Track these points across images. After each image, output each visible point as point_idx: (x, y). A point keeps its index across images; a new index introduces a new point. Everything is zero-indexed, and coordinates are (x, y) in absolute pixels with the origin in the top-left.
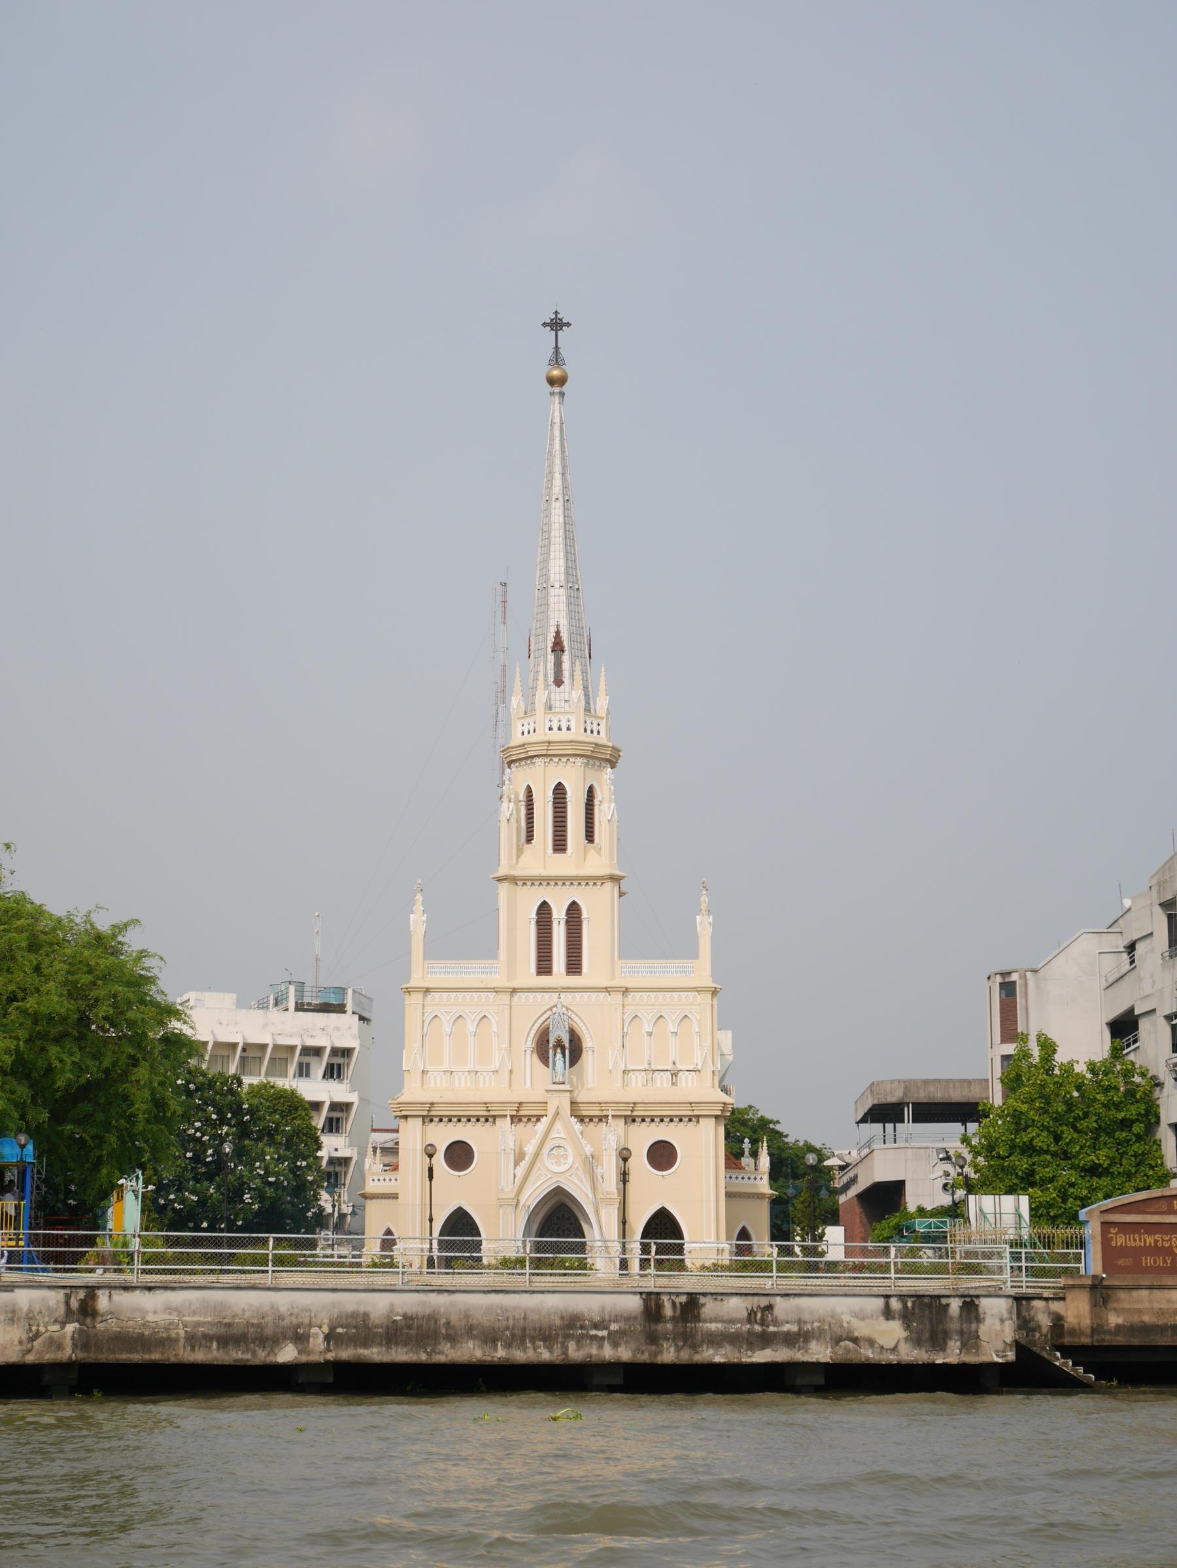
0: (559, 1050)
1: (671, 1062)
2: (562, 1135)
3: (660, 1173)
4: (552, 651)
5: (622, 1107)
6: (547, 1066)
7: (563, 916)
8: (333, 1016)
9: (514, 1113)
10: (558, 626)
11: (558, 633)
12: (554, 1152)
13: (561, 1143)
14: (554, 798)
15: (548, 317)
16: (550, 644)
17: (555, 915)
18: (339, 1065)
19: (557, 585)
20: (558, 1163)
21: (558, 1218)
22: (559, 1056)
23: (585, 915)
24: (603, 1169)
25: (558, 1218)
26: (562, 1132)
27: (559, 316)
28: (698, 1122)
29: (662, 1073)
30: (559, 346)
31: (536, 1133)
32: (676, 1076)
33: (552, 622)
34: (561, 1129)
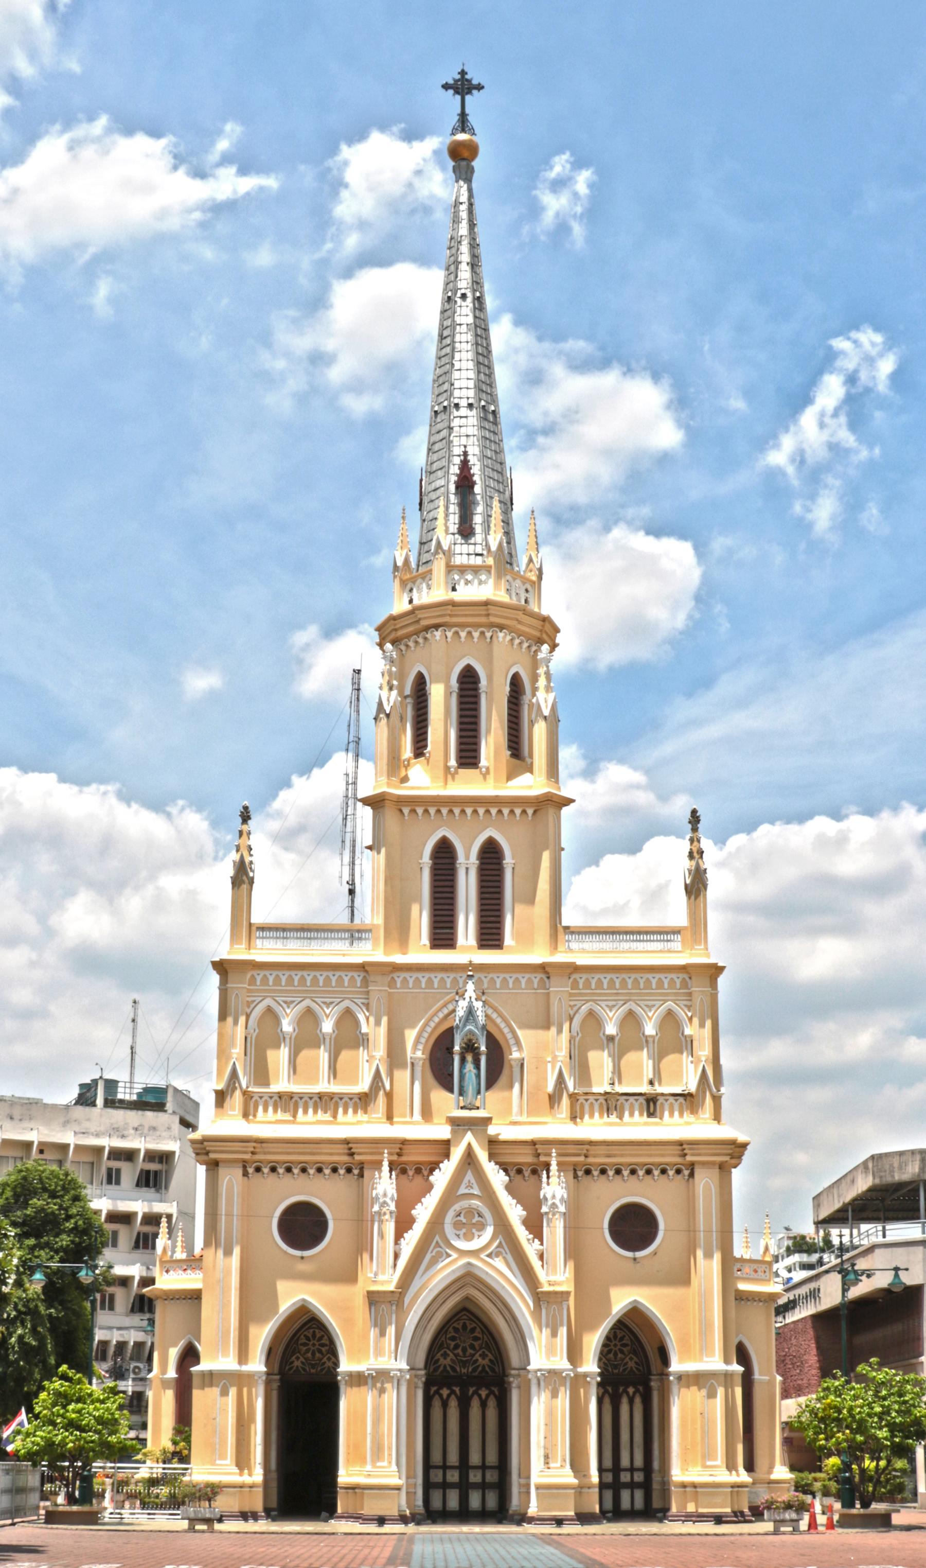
0: (469, 1058)
1: (646, 1081)
2: (476, 1191)
3: (630, 1254)
4: (457, 488)
5: (572, 1149)
6: (451, 1090)
7: (474, 860)
8: (149, 1114)
9: (395, 1158)
10: (465, 454)
11: (465, 465)
12: (462, 1218)
13: (476, 1203)
14: (461, 689)
15: (451, 76)
16: (453, 478)
17: (461, 858)
18: (156, 1172)
19: (464, 403)
20: (469, 1237)
21: (456, 1330)
22: (470, 1066)
23: (508, 860)
24: (542, 1244)
25: (456, 1330)
26: (475, 1186)
27: (467, 77)
28: (692, 1175)
29: (632, 1099)
30: (467, 111)
31: (430, 1187)
32: (655, 1104)
33: (457, 451)
34: (473, 1181)
